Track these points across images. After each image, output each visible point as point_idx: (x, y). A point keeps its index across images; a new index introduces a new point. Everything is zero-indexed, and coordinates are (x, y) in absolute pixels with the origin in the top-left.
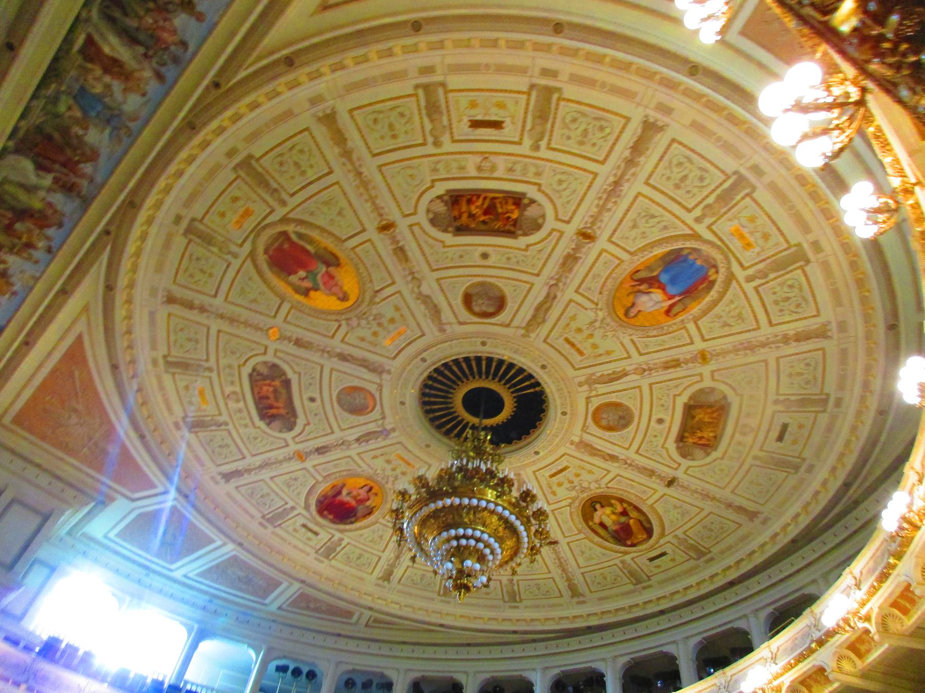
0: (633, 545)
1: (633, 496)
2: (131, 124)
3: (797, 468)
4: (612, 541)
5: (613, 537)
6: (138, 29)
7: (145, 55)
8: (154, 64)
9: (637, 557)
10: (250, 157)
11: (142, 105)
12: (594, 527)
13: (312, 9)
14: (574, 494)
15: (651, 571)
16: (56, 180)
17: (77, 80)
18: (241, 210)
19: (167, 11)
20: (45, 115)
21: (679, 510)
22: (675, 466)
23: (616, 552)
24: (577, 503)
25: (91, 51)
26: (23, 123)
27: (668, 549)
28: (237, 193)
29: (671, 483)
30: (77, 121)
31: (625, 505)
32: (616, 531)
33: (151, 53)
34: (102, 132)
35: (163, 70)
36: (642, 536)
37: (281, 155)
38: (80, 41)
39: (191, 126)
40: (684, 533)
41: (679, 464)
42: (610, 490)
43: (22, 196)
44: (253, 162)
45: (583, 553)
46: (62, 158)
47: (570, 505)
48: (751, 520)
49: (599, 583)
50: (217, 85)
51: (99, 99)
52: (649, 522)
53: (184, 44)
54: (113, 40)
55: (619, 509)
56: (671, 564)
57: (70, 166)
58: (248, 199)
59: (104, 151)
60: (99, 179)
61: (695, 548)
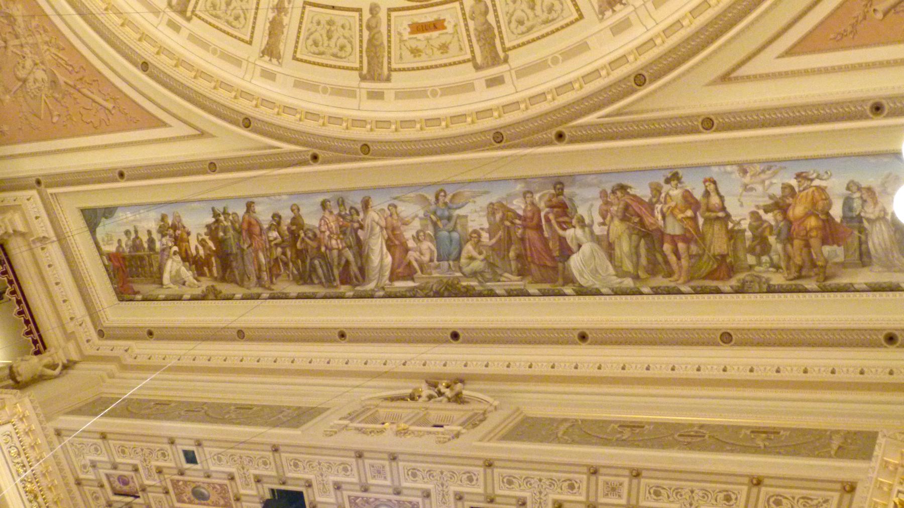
2: (432, 198)
6: (350, 247)
7: (361, 227)
8: (362, 215)
10: (363, 78)
11: (404, 201)
13: (209, 140)
16: (564, 226)
17: (437, 267)
18: (420, 36)
19: (315, 235)
20: (501, 275)
25: (403, 270)
26: (532, 289)
28: (407, 54)
30: (478, 243)
33: (356, 225)
34: (466, 217)
35: (359, 206)
37: (335, 55)
38: (400, 284)
39: (366, 149)
43: (624, 247)
44: (365, 71)
46: (531, 234)
50: (315, 158)
51: (436, 239)
53: (324, 205)
54: (375, 259)
57: (533, 222)
58: (401, 41)
59: (483, 202)
60: (519, 187)
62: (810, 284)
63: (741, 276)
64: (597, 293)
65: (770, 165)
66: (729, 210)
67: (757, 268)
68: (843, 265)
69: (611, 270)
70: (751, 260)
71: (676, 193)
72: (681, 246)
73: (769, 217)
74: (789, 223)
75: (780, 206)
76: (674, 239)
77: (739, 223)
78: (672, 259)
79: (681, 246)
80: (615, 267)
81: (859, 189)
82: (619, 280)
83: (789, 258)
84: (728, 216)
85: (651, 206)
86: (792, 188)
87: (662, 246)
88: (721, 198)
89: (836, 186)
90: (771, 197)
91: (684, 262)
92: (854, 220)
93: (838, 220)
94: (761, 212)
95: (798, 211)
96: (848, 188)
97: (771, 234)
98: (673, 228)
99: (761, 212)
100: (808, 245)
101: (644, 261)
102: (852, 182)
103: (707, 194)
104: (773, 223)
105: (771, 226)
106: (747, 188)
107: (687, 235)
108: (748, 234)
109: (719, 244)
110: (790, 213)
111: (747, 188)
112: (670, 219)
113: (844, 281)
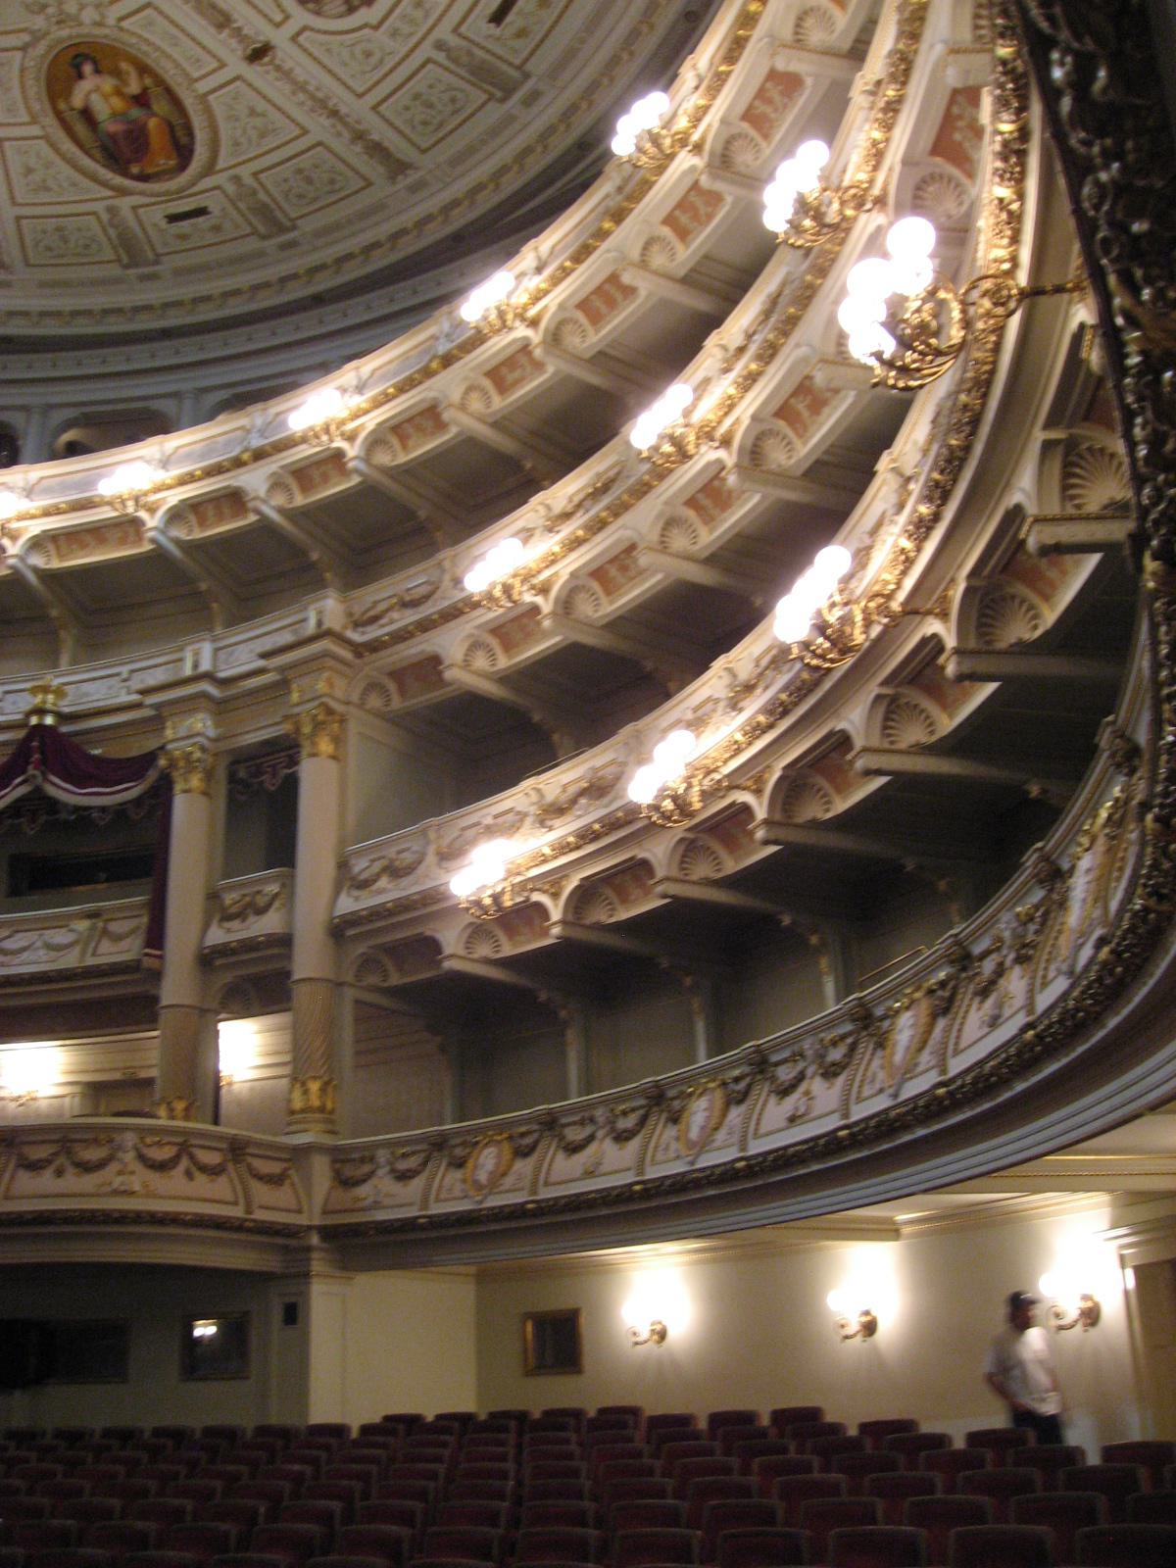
0: (143, 178)
1: (169, 66)
3: (508, 92)
4: (98, 155)
5: (104, 148)
9: (143, 206)
12: (68, 115)
14: (39, 22)
15: (166, 244)
21: (258, 122)
22: (278, 17)
23: (104, 184)
24: (41, 48)
27: (213, 202)
29: (259, 54)
31: (148, 81)
32: (113, 137)
36: (165, 161)
40: (255, 174)
41: (287, 17)
42: (126, 37)
45: (29, 171)
47: (24, 48)
48: (392, 178)
49: (49, 249)
52: (191, 134)
55: (134, 87)
56: (211, 238)
61: (264, 211)
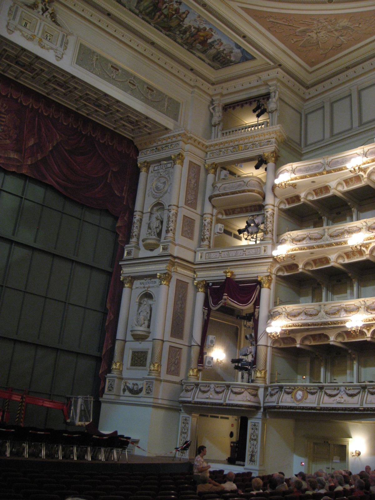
62: (185, 47)
63: (170, 33)
64: (125, 7)
65: (207, 22)
66: (185, 20)
67: (177, 35)
68: (198, 50)
69: (135, 5)
70: (178, 33)
71: (176, 6)
72: (163, 16)
73: (193, 30)
74: (196, 34)
75: (198, 30)
76: (162, 14)
77: (184, 24)
78: (157, 17)
79: (163, 16)
80: (137, 5)
81: (220, 42)
82: (134, 9)
83: (188, 39)
84: (183, 21)
85: (165, 3)
86: (206, 29)
87: (157, 12)
88: (186, 17)
89: (216, 37)
90: (198, 26)
91: (159, 20)
92: (211, 45)
93: (208, 42)
94: (192, 27)
95: (201, 34)
96: (218, 40)
97: (189, 32)
98: (165, 12)
99: (192, 27)
100: (195, 41)
101: (147, 11)
102: (221, 39)
103: (184, 13)
104: (192, 31)
105: (191, 31)
106: (195, 20)
107: (167, 16)
108: (184, 28)
109: (174, 24)
110: (199, 33)
111: (195, 20)
112: (166, 10)
113: (194, 52)
